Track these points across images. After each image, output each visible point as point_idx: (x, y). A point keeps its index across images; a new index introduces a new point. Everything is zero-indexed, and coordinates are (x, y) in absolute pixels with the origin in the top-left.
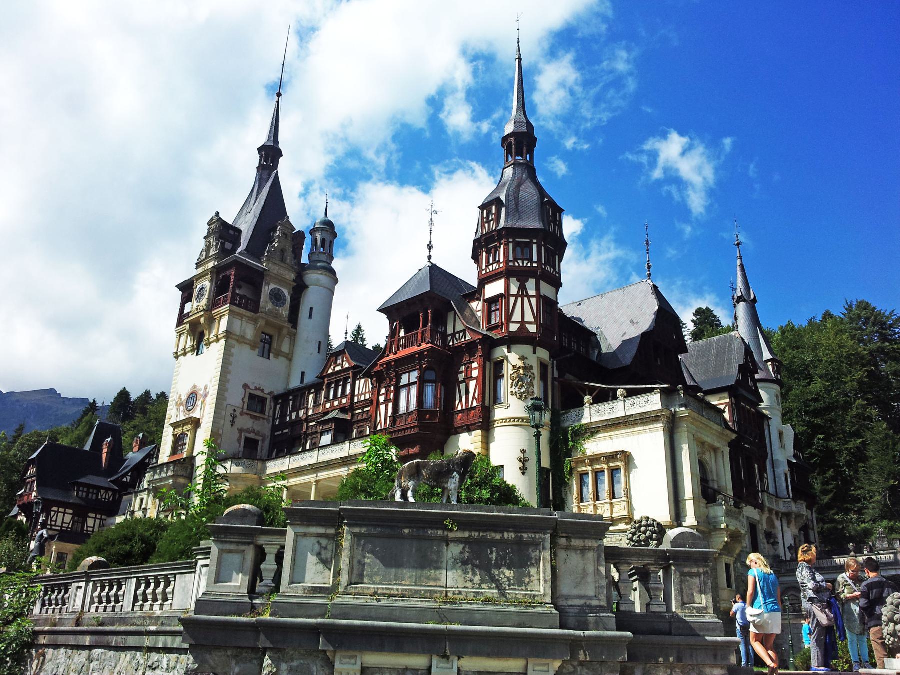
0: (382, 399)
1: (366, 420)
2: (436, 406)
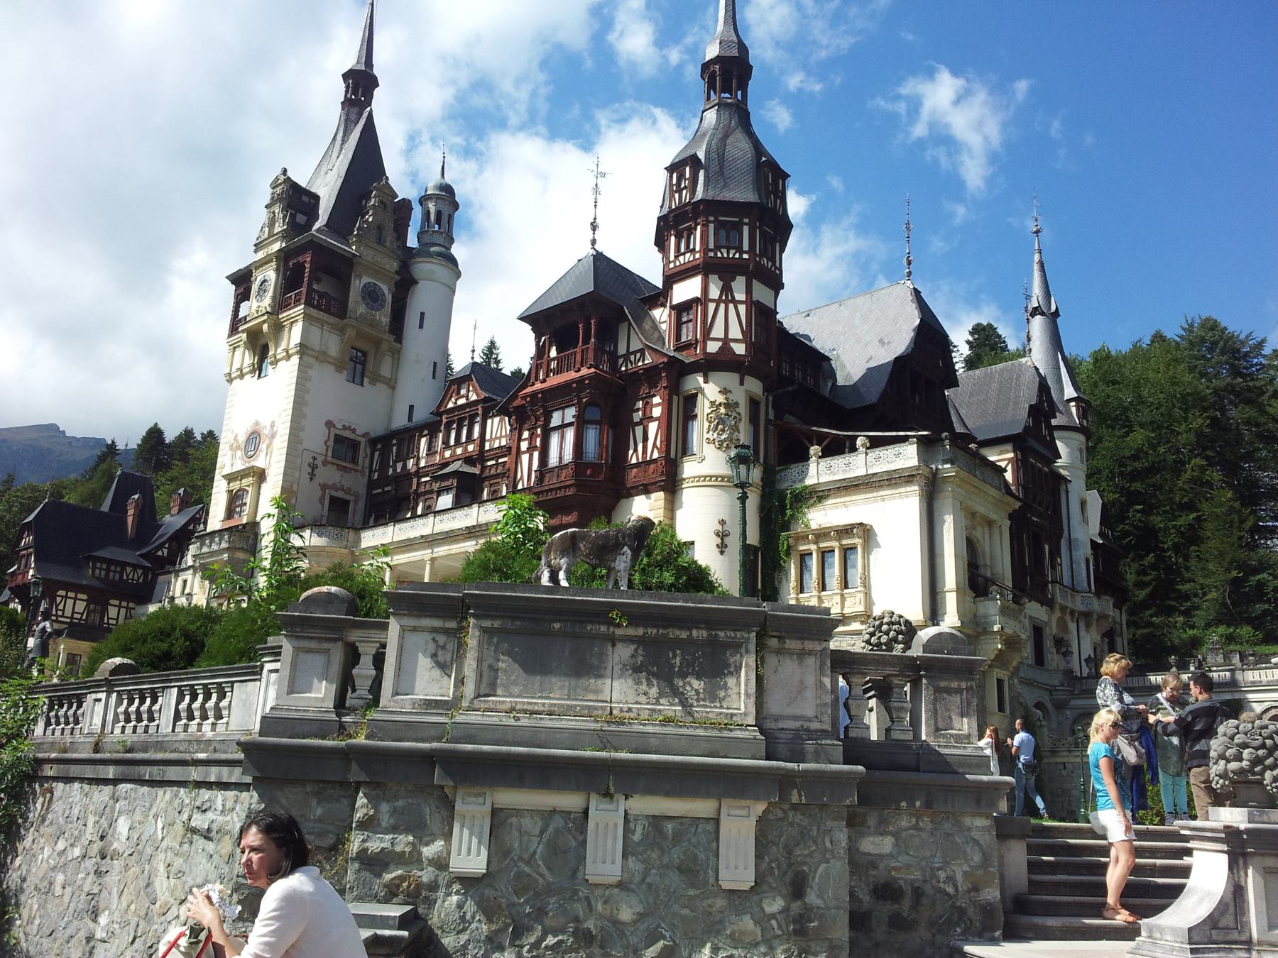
0: (524, 446)
1: (502, 475)
2: (600, 457)
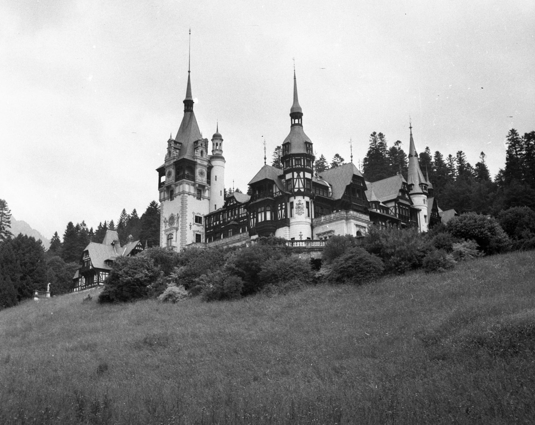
0: (252, 217)
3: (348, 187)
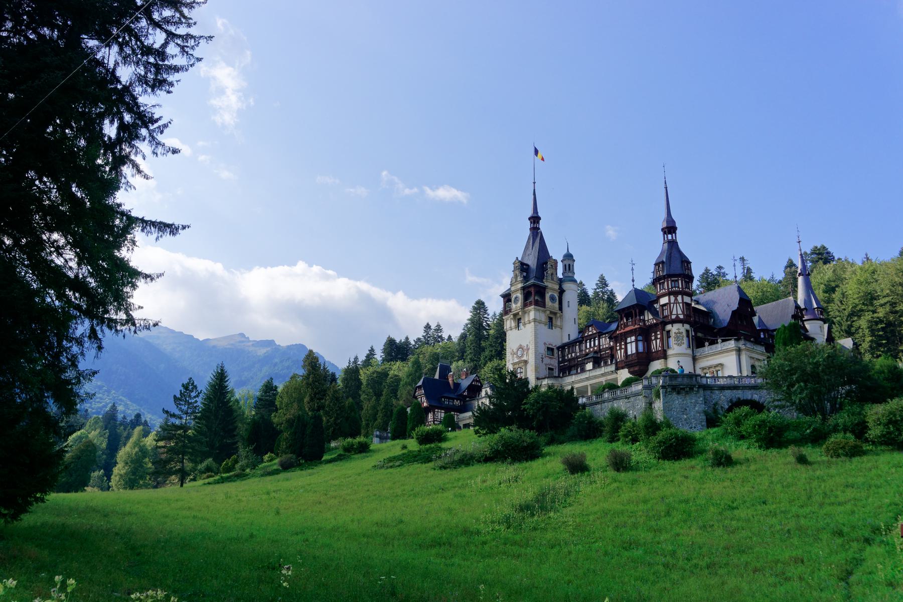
3: (734, 312)
